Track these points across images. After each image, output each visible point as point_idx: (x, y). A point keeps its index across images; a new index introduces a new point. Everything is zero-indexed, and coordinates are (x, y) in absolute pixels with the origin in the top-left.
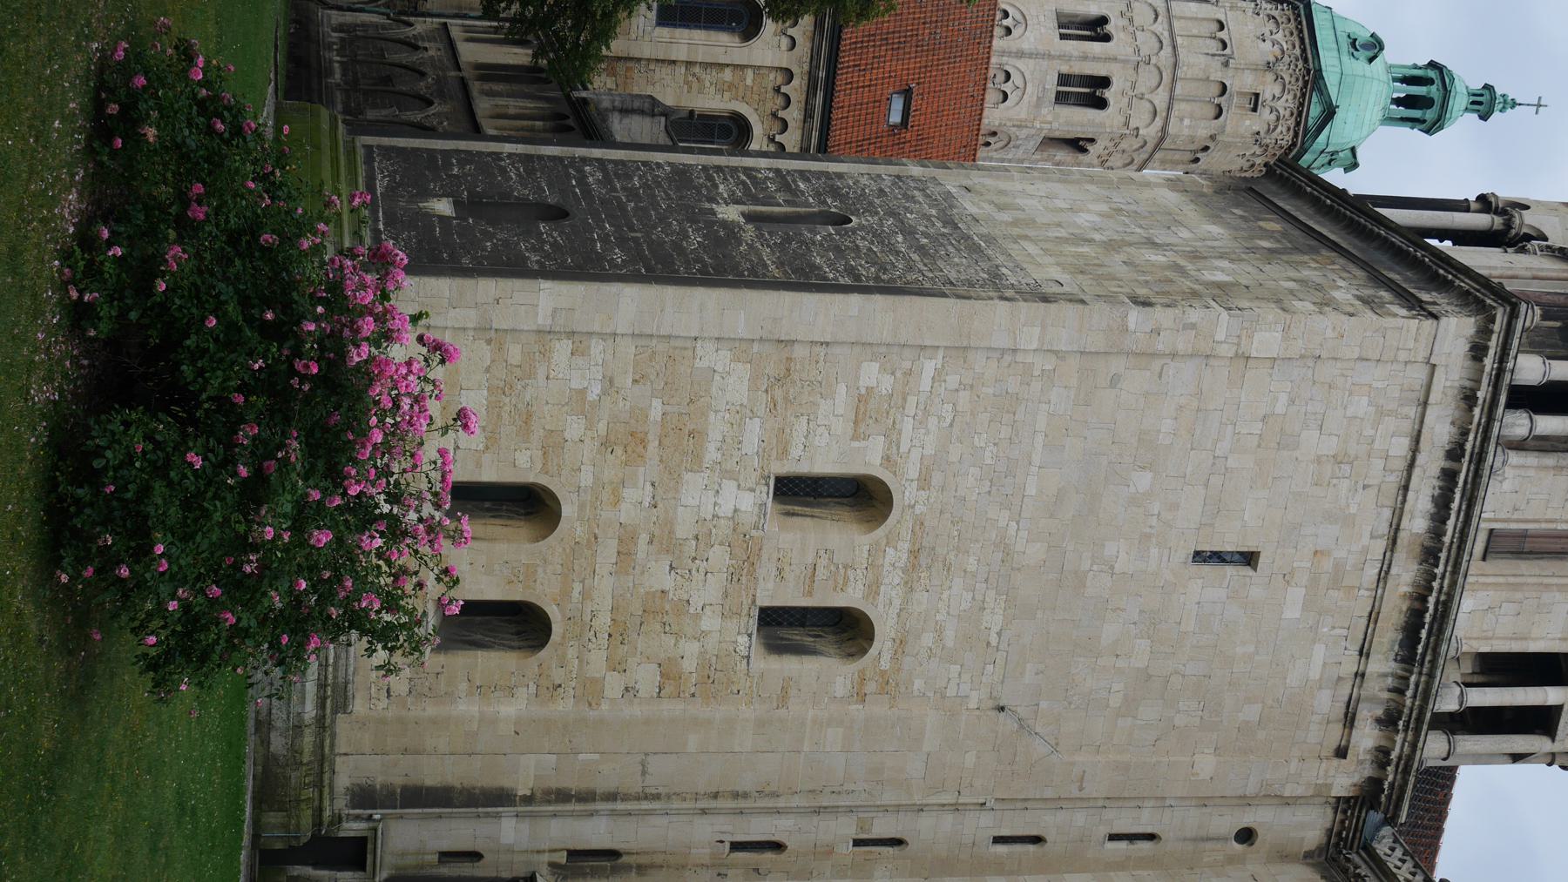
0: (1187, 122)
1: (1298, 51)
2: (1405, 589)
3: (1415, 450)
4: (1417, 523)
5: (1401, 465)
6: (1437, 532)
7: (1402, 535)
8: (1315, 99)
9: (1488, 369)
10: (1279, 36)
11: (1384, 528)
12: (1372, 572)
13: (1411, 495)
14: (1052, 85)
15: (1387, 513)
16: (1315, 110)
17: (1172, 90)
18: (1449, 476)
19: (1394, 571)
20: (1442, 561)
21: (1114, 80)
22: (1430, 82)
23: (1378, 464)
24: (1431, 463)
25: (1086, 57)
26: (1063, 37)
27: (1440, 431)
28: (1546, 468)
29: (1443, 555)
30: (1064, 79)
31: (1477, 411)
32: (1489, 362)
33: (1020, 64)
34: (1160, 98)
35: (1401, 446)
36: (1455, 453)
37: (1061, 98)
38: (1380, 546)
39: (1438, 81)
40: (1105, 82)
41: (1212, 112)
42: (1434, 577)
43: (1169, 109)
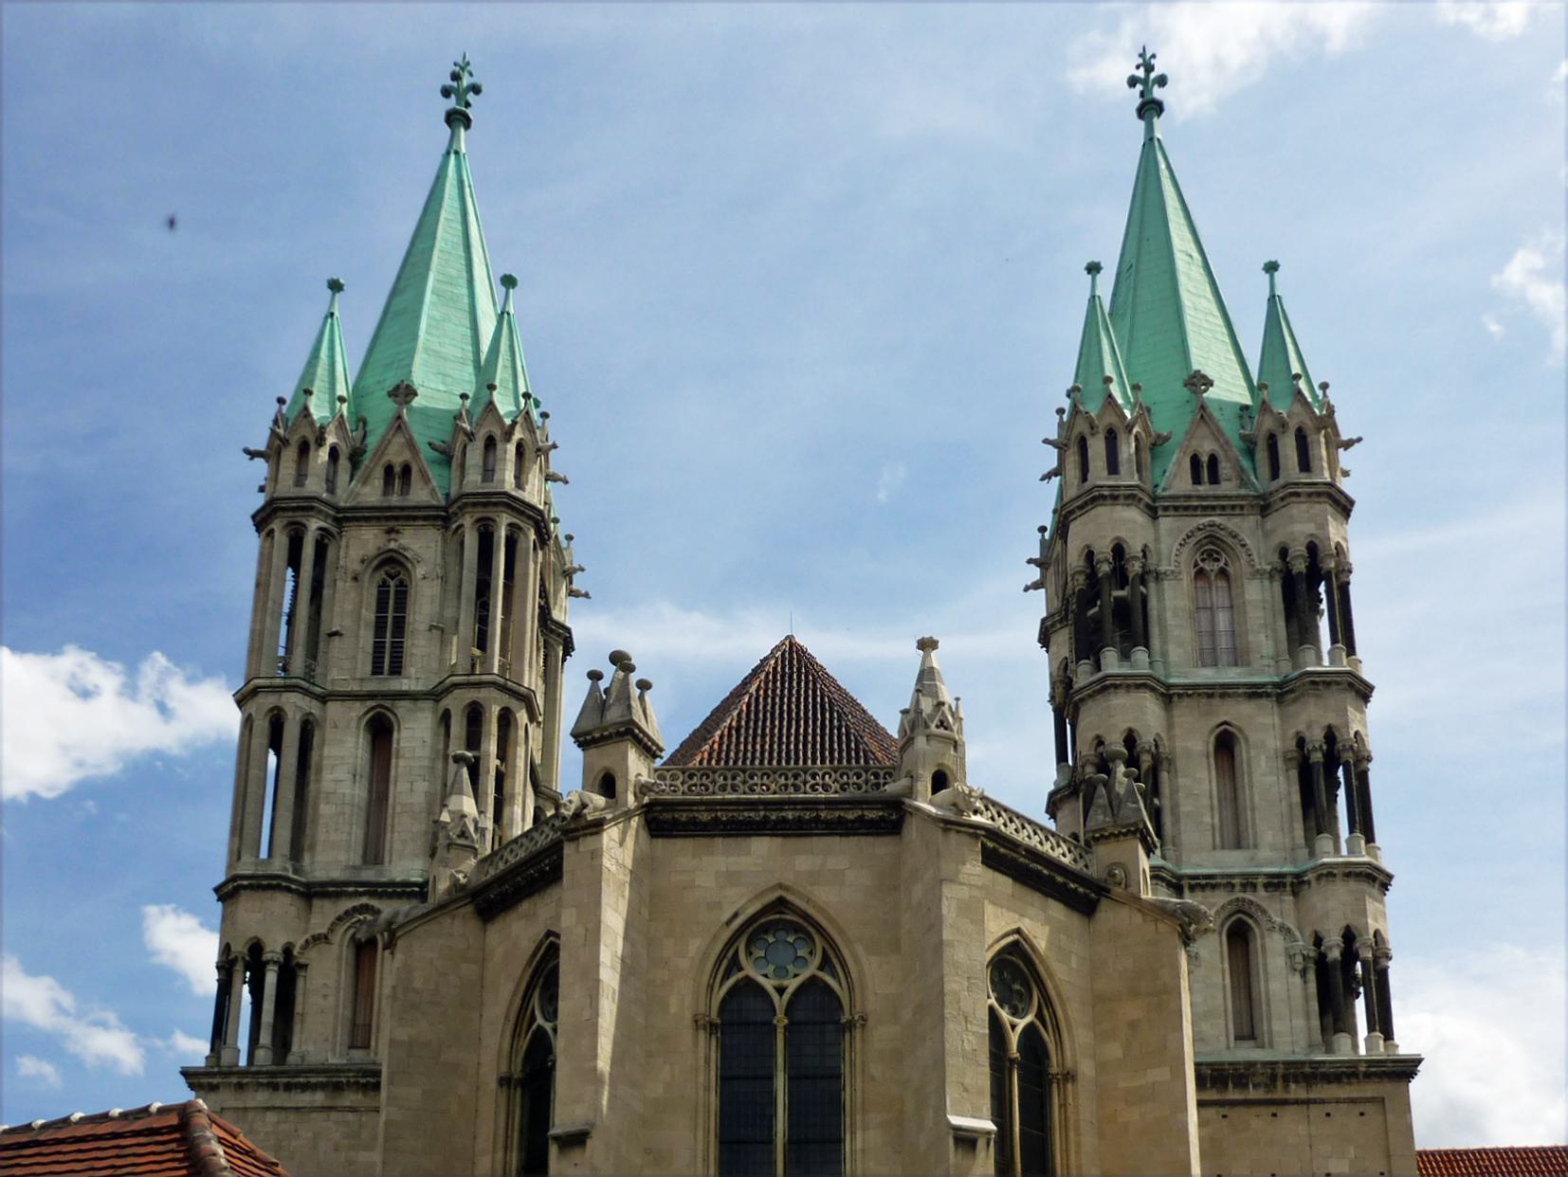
2: (360, 1096)
3: (274, 1108)
4: (319, 1098)
5: (283, 1115)
6: (322, 1086)
7: (326, 1104)
9: (220, 1080)
11: (324, 1115)
12: (350, 1116)
13: (300, 1105)
15: (314, 1115)
18: (288, 1087)
19: (347, 1103)
20: (339, 1079)
23: (282, 1127)
24: (281, 1099)
27: (262, 1097)
28: (302, 1028)
29: (334, 1080)
31: (245, 1081)
32: (215, 1081)
35: (271, 1117)
36: (275, 1087)
38: (334, 1115)
42: (348, 1082)
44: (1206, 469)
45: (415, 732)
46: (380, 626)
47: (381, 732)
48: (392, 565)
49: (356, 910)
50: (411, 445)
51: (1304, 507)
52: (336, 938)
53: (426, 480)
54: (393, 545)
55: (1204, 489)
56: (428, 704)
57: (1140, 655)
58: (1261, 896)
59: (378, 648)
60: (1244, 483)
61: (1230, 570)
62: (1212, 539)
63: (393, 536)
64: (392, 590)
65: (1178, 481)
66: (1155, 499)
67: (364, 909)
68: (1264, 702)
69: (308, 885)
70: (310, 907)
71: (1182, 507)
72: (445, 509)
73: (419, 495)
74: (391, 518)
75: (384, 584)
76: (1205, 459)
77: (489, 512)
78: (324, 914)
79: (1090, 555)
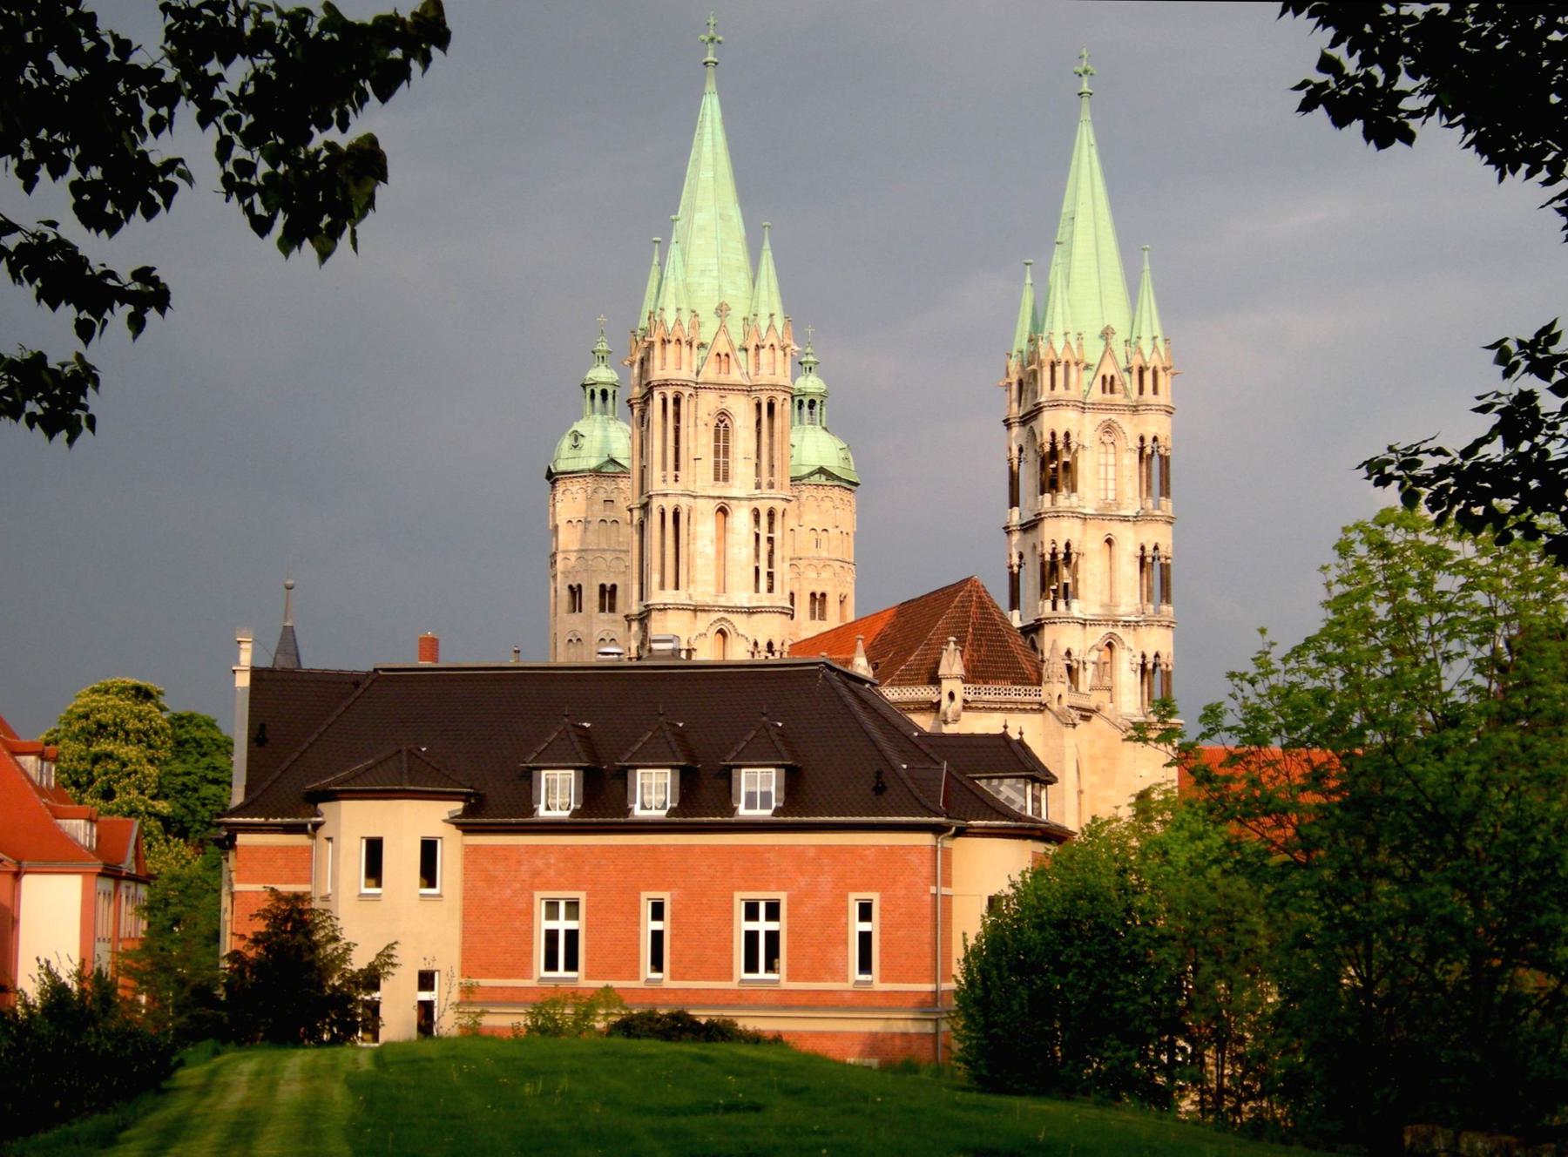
0: (621, 539)
1: (580, 480)
8: (604, 470)
10: (574, 489)
14: (606, 616)
16: (611, 469)
17: (604, 550)
21: (601, 582)
22: (593, 391)
25: (591, 597)
26: (580, 611)
30: (602, 609)
33: (596, 634)
34: (609, 556)
37: (612, 609)
39: (592, 387)
40: (603, 587)
41: (615, 524)
43: (614, 551)
44: (1109, 384)
45: (741, 518)
46: (717, 453)
47: (723, 511)
48: (723, 415)
49: (719, 620)
50: (730, 343)
51: (1154, 416)
52: (709, 635)
53: (739, 367)
54: (724, 406)
55: (1108, 396)
56: (745, 503)
57: (1074, 497)
58: (1119, 631)
59: (717, 464)
60: (1126, 396)
61: (1116, 443)
62: (1109, 426)
63: (723, 400)
64: (722, 429)
65: (1096, 395)
66: (1084, 404)
67: (723, 619)
68: (1127, 523)
69: (696, 606)
70: (696, 616)
71: (1096, 407)
72: (750, 387)
73: (736, 377)
74: (724, 388)
75: (717, 426)
76: (1108, 379)
77: (774, 394)
78: (704, 622)
79: (1053, 435)
